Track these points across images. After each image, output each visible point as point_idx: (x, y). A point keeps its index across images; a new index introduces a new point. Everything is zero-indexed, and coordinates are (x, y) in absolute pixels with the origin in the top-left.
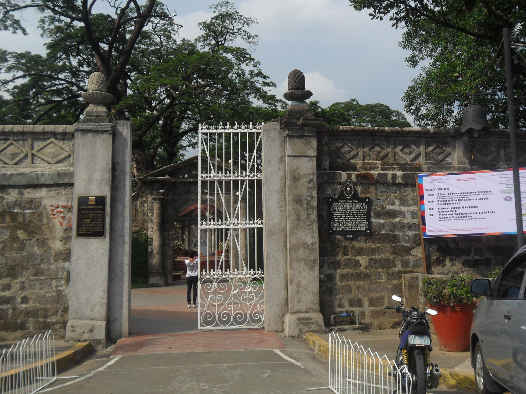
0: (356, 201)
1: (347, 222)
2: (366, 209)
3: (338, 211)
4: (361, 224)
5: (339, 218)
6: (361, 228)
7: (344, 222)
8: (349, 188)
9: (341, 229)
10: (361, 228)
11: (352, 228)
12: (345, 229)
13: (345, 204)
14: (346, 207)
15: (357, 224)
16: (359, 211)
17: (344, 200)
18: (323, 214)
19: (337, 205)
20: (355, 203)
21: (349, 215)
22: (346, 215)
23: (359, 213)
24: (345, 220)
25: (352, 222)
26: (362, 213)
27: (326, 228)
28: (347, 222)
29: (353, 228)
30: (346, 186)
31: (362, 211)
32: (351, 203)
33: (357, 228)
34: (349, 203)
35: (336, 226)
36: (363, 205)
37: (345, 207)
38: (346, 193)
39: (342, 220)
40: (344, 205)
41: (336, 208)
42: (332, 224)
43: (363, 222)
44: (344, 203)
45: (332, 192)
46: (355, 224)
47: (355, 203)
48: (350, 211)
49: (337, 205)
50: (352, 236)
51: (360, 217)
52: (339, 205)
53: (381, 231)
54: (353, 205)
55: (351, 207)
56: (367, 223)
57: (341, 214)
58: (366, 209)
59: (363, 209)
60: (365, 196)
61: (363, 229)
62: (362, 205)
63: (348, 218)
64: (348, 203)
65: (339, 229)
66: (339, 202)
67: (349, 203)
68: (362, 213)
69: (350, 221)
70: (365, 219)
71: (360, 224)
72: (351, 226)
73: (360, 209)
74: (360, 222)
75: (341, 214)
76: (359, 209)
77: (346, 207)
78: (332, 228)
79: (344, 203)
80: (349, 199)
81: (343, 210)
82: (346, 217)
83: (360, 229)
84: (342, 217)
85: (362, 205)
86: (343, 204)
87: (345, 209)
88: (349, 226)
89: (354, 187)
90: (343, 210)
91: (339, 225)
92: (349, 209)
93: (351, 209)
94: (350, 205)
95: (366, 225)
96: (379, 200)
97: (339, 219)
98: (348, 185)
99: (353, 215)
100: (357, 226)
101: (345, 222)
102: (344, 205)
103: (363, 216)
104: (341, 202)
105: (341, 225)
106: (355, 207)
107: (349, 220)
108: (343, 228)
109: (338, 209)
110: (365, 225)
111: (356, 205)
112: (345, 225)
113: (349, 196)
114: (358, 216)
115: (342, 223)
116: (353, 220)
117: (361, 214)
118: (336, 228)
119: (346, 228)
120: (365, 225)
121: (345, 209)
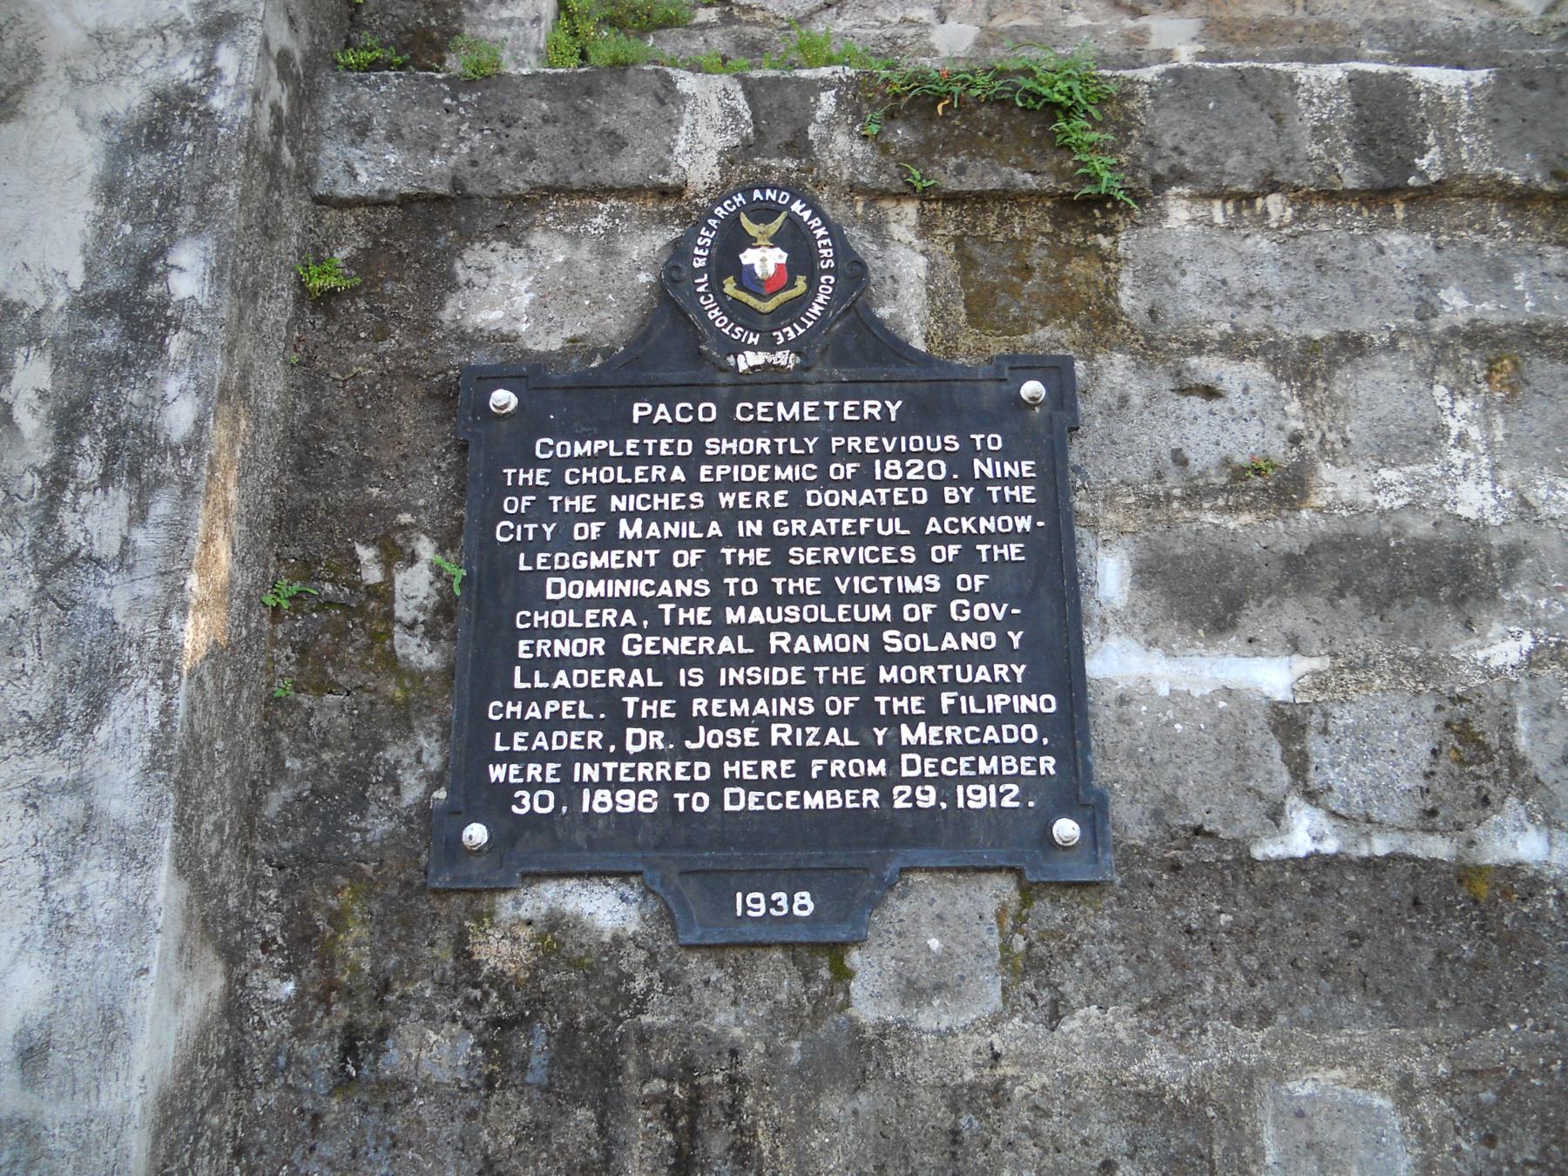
0: (872, 408)
1: (739, 691)
2: (1016, 508)
3: (609, 539)
4: (956, 716)
5: (613, 635)
6: (946, 786)
7: (683, 698)
8: (776, 241)
9: (645, 802)
10: (946, 786)
11: (803, 781)
12: (701, 803)
13: (712, 446)
14: (729, 485)
15: (893, 721)
16: (923, 543)
17: (696, 390)
18: (384, 593)
19: (601, 459)
20: (865, 427)
21: (767, 598)
22: (718, 601)
23: (924, 565)
24: (711, 664)
25: (819, 689)
26: (968, 560)
27: (413, 789)
28: (739, 691)
29: (826, 781)
30: (732, 221)
31: (969, 541)
32: (795, 428)
33: (884, 785)
34: (776, 429)
35: (566, 759)
36: (969, 451)
37: (711, 491)
38: (735, 310)
39: (666, 666)
40: (690, 465)
41: (583, 503)
42: (509, 727)
43: (980, 692)
44: (698, 432)
45: (540, 304)
46: (864, 717)
47: (865, 427)
48: (779, 548)
49: (601, 459)
50: (804, 903)
51: (940, 624)
52: (628, 464)
53: (1276, 815)
54: (824, 457)
55: (796, 489)
56: (1046, 703)
57: (641, 588)
58: (1016, 508)
59: (981, 506)
60: (997, 346)
61: (978, 798)
62: (960, 466)
63: (757, 635)
64: (755, 430)
65: (599, 802)
66: (620, 428)
67: (776, 429)
68: (968, 560)
69: (777, 676)
70: (1004, 652)
71: (933, 715)
72: (802, 756)
73: (938, 507)
74: (930, 692)
75: (641, 588)
76: (914, 517)
77: (729, 485)
78: (505, 792)
79: (698, 432)
80: (769, 383)
81: (690, 530)
82: (718, 629)
83: (928, 799)
84: (658, 629)
85: (960, 466)
86: (686, 447)
87: (712, 510)
88: (764, 750)
89: (834, 232)
90: (690, 530)
91: (615, 735)
92: (767, 515)
93: (798, 506)
94: (787, 459)
95: (1030, 733)
96: (1210, 393)
97: (613, 657)
98: (764, 213)
99: (830, 597)
100: (892, 750)
101: (711, 689)
102: (700, 456)
103: (983, 612)
104: (648, 428)
105: (637, 739)
106: (863, 480)
107: (765, 658)
108: (667, 788)
109: (601, 510)
110: (1012, 734)
111: (865, 460)
112: (707, 738)
113: (769, 345)
114: (898, 599)
115: (664, 709)
116: (831, 658)
117: (948, 572)
118: (568, 790)
119: (715, 786)
120: (1012, 734)
121: (712, 510)
